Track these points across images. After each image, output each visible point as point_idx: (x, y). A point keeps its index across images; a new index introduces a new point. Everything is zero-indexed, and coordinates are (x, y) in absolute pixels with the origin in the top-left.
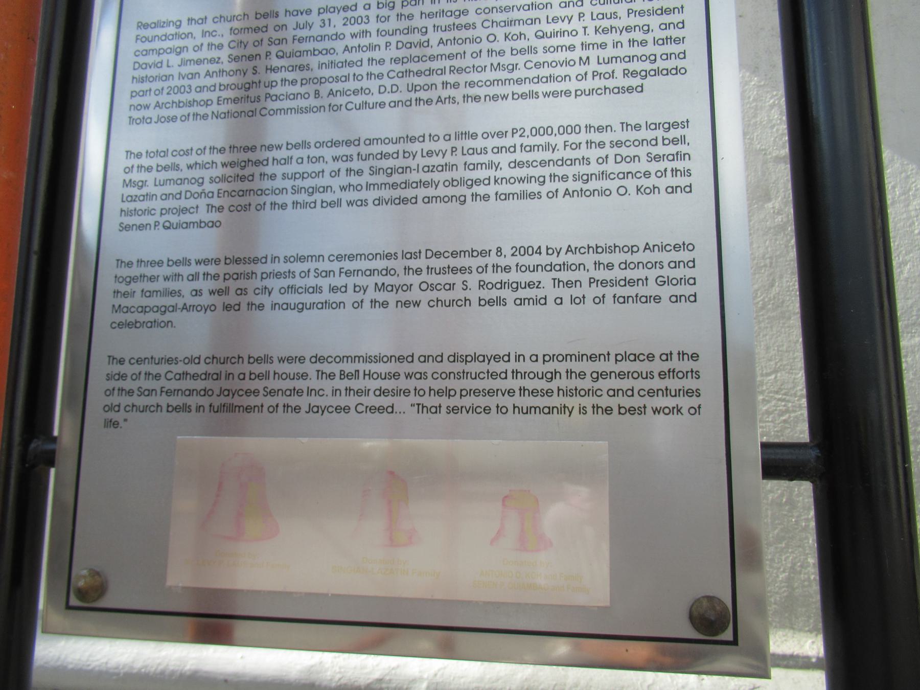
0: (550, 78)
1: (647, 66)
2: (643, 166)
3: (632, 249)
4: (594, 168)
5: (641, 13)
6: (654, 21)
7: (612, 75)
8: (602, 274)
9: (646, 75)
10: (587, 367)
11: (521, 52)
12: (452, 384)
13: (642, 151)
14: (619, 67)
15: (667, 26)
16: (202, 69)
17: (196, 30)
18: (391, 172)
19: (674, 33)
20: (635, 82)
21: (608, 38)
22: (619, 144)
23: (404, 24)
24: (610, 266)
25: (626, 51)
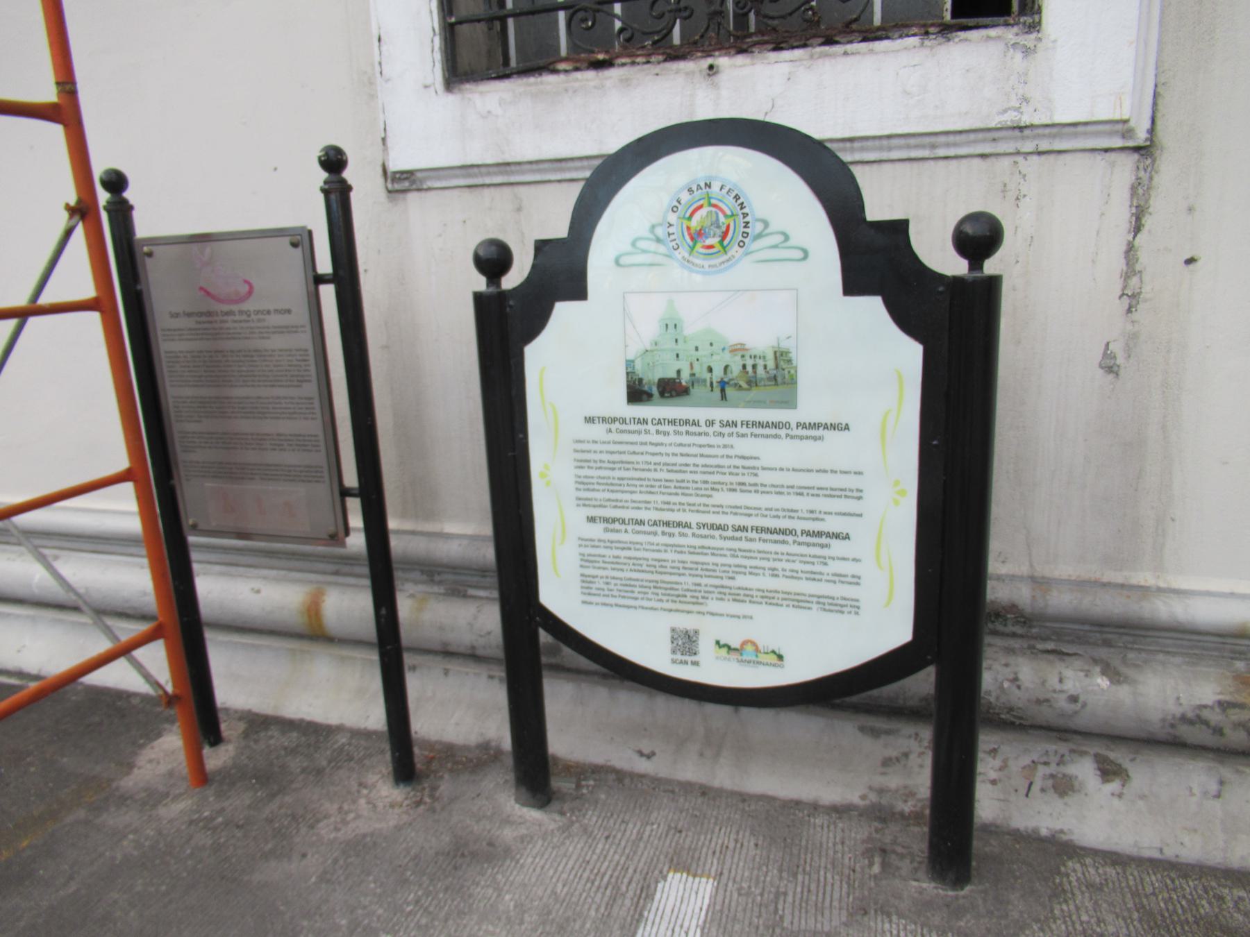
0: (278, 381)
1: (302, 379)
2: (303, 411)
3: (304, 436)
4: (292, 411)
5: (299, 361)
6: (303, 363)
7: (293, 381)
8: (298, 443)
9: (301, 381)
10: (298, 469)
11: (270, 371)
12: (267, 472)
13: (304, 406)
14: (295, 379)
15: (306, 366)
16: (187, 369)
17: (181, 355)
18: (243, 408)
19: (307, 368)
20: (299, 384)
21: (292, 368)
22: (298, 403)
23: (238, 359)
24: (299, 440)
25: (296, 373)
